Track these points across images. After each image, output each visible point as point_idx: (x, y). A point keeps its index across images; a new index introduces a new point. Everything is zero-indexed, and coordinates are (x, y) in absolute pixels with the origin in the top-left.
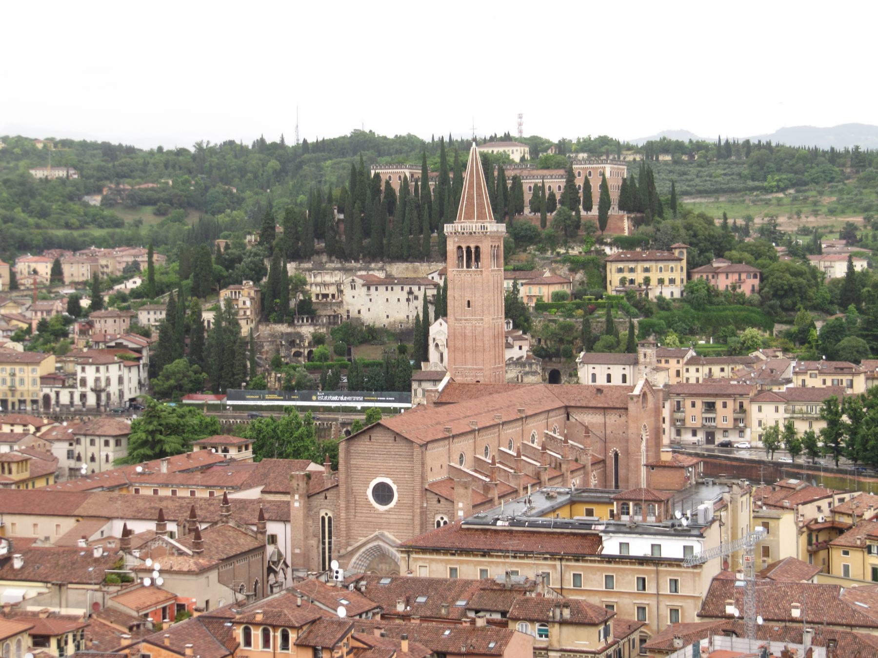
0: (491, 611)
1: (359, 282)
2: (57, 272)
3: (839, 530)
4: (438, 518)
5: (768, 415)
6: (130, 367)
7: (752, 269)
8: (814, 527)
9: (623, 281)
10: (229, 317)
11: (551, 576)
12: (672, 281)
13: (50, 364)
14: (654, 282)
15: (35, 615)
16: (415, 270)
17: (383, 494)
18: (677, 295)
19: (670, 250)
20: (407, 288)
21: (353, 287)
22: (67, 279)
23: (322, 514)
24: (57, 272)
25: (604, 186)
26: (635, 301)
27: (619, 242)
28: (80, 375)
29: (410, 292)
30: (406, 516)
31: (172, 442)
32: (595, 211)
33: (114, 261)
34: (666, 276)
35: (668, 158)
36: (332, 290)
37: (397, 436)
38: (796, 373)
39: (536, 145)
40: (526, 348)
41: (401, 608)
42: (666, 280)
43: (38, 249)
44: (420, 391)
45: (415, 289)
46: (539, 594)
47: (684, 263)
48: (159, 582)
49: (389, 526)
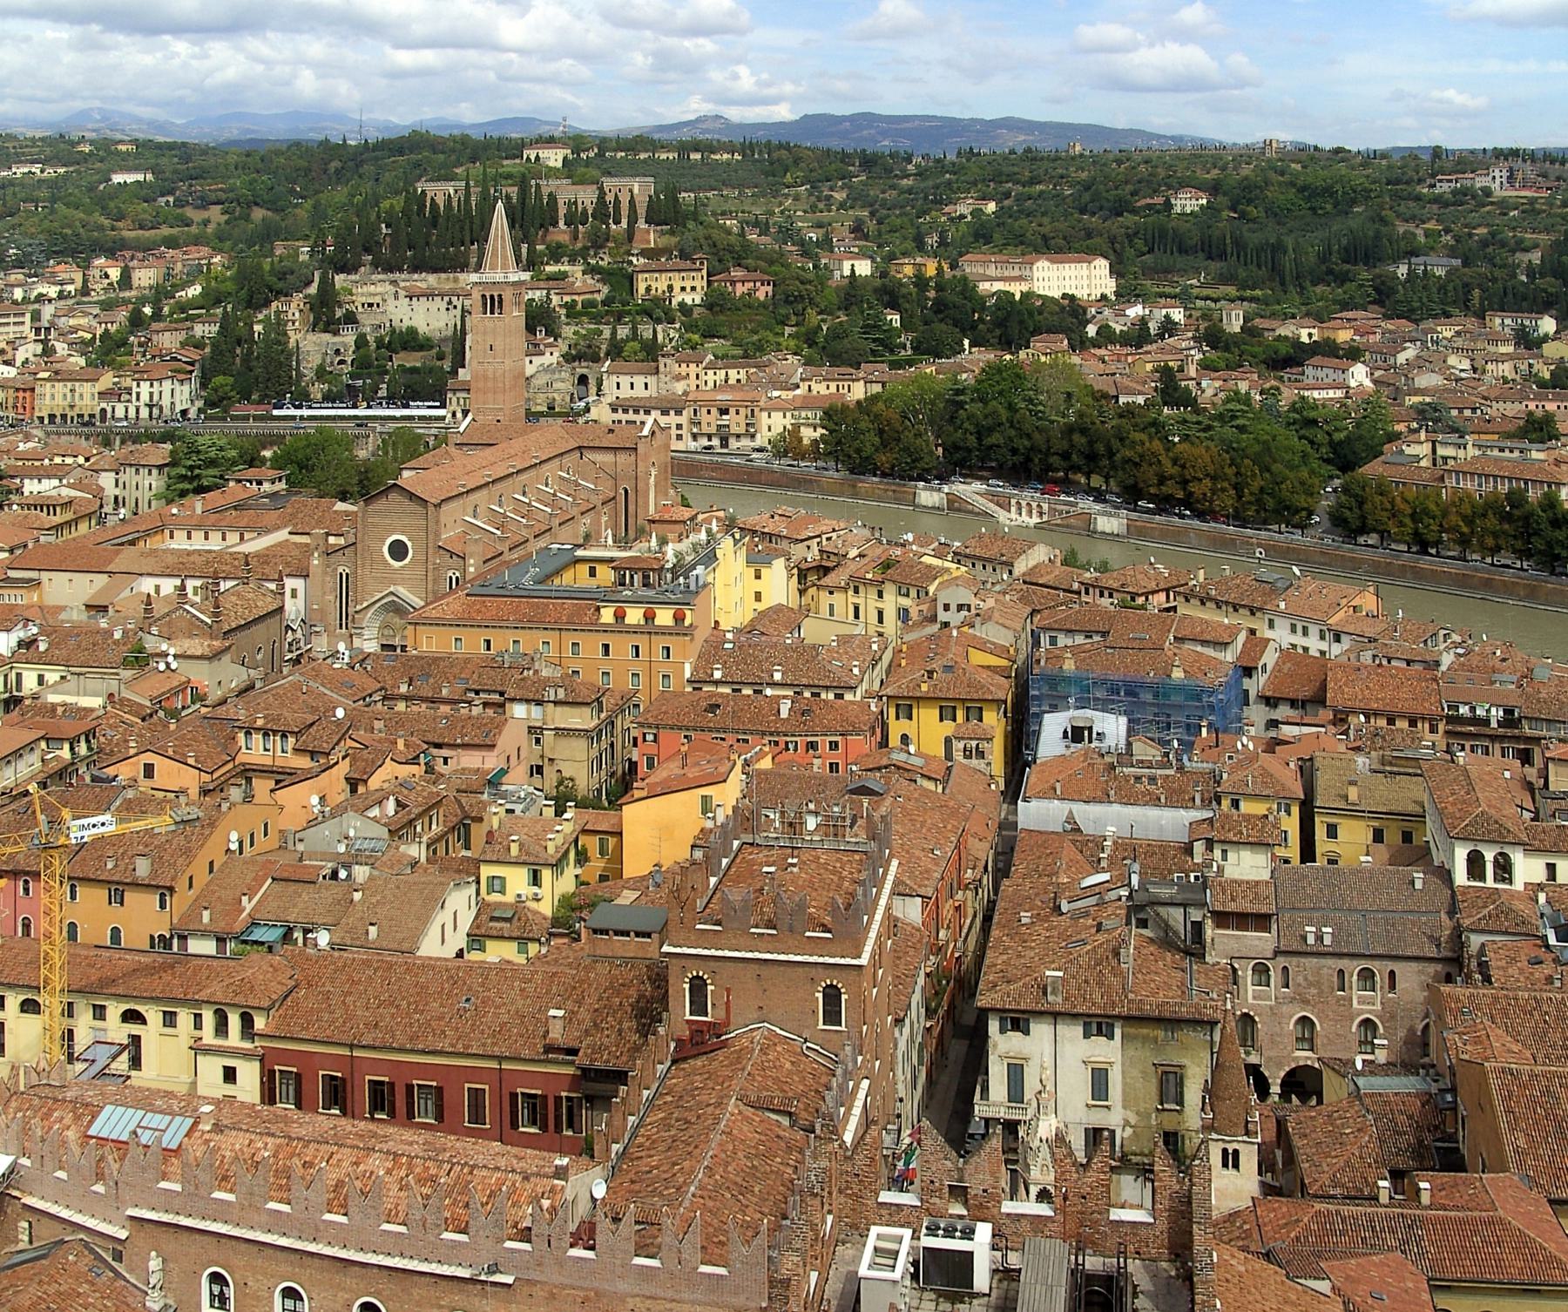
0: (489, 692)
1: (402, 293)
2: (126, 281)
3: (826, 571)
4: (450, 573)
5: (774, 424)
6: (182, 382)
7: (766, 277)
8: (804, 566)
9: (648, 289)
10: (278, 327)
11: (546, 651)
12: (693, 289)
13: (108, 380)
14: (677, 289)
15: (54, 707)
16: (456, 280)
17: (398, 550)
18: (698, 301)
19: (693, 261)
20: (446, 299)
21: (396, 298)
22: (135, 283)
23: (340, 570)
24: (126, 281)
25: (632, 202)
26: (657, 309)
27: (644, 253)
28: (135, 390)
29: (450, 303)
30: (421, 572)
31: (208, 476)
32: (624, 224)
33: (181, 261)
34: (688, 284)
35: (698, 156)
36: (377, 299)
37: (412, 496)
38: (802, 380)
39: (577, 142)
40: (556, 354)
41: (404, 689)
42: (689, 289)
43: (111, 252)
44: (454, 400)
45: (454, 299)
46: (536, 672)
47: (704, 272)
48: (174, 666)
49: (402, 582)
